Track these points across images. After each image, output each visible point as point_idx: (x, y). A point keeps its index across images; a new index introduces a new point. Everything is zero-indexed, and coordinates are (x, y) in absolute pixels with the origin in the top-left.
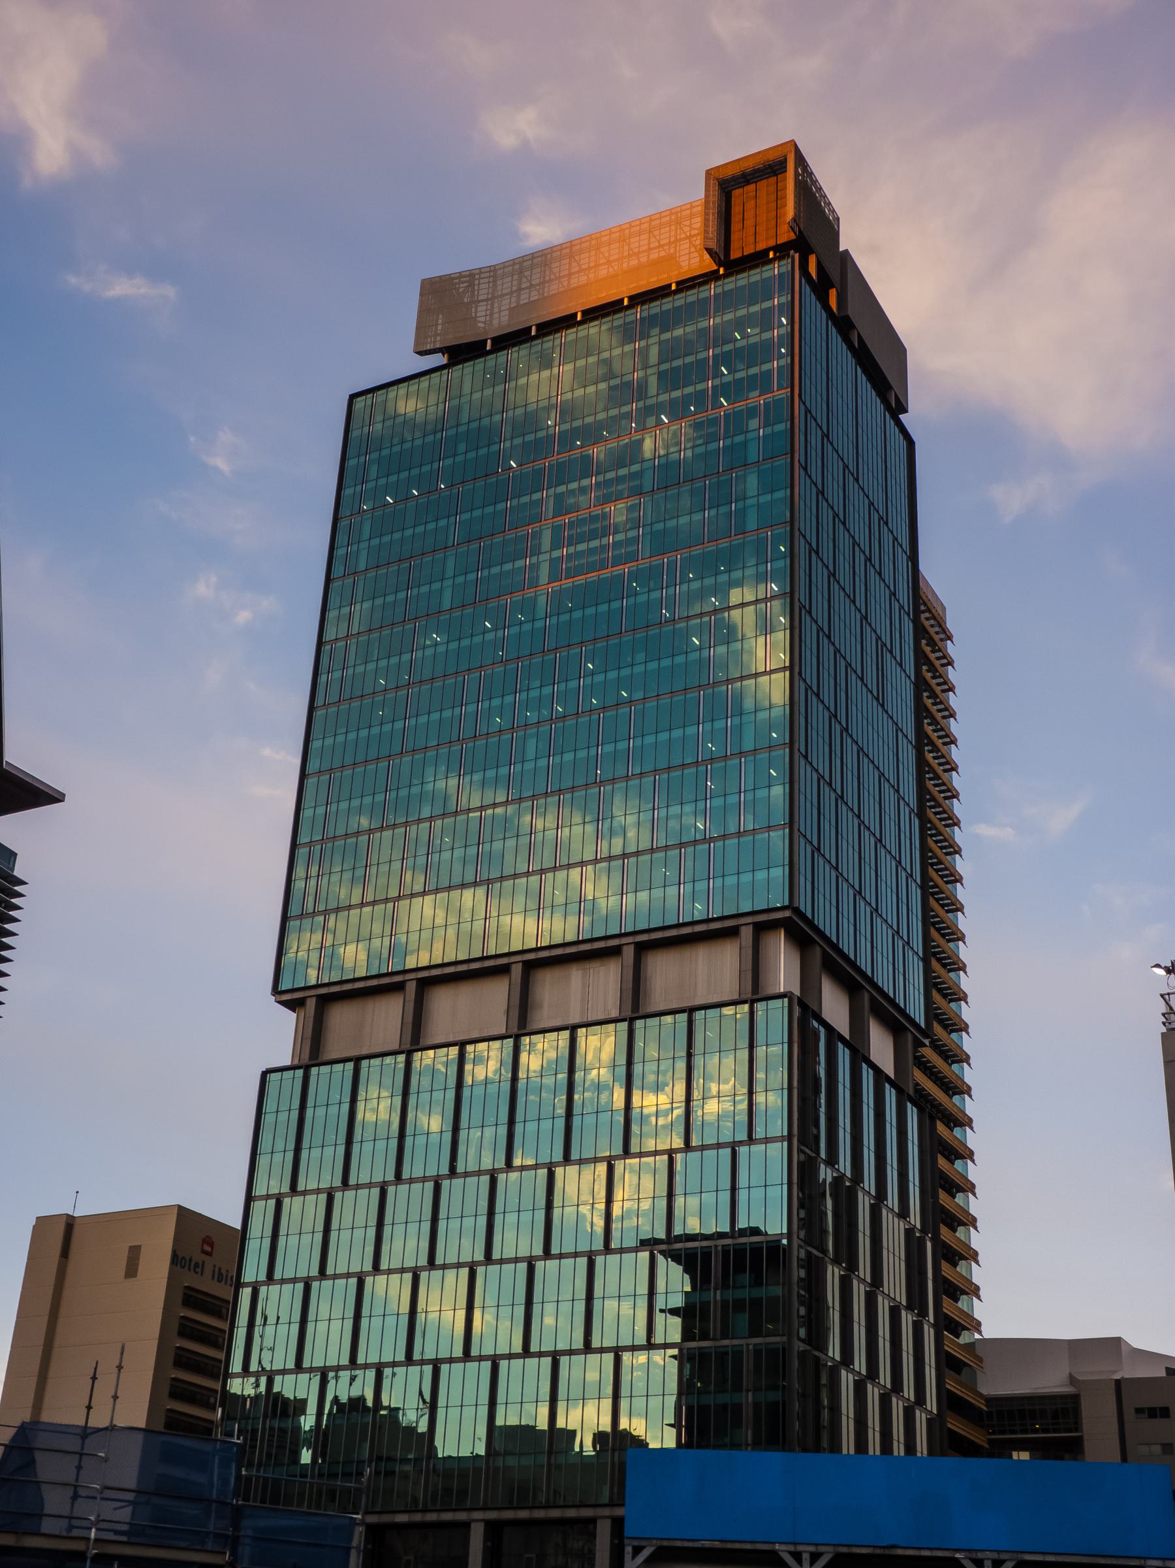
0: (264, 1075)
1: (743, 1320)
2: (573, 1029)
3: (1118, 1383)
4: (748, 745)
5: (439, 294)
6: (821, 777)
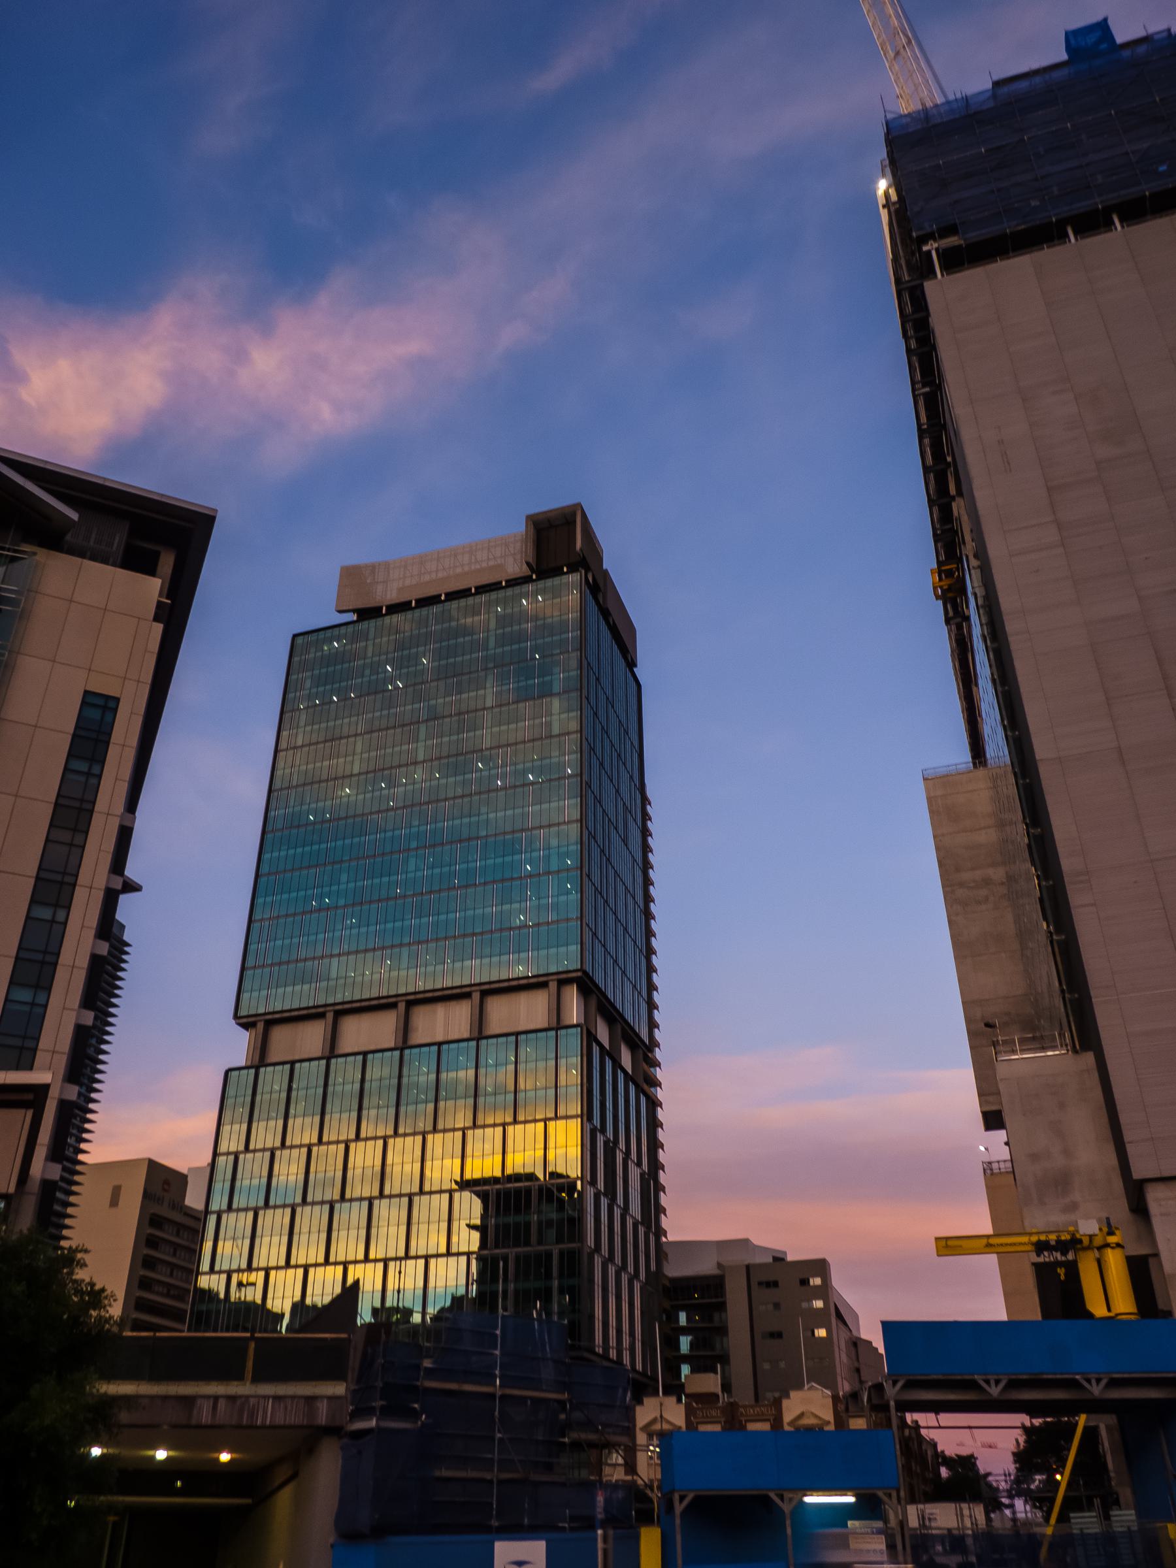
0: (227, 1072)
1: (552, 1234)
2: (440, 1044)
3: (748, 1267)
4: (554, 867)
6: (596, 889)
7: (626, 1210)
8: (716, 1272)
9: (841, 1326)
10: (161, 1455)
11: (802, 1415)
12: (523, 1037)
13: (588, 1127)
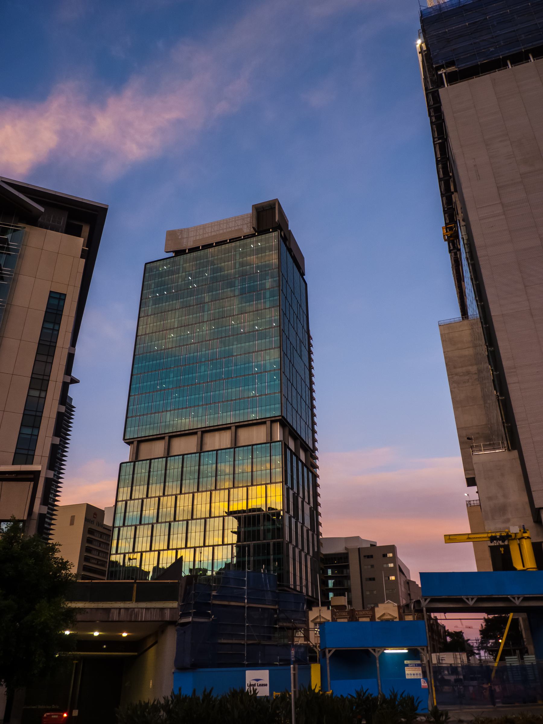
0: (121, 464)
1: (270, 535)
2: (217, 450)
3: (359, 549)
5: (172, 235)
6: (288, 379)
7: (303, 523)
8: (345, 551)
9: (401, 574)
10: (67, 633)
11: (384, 614)
12: (255, 447)
13: (285, 487)
